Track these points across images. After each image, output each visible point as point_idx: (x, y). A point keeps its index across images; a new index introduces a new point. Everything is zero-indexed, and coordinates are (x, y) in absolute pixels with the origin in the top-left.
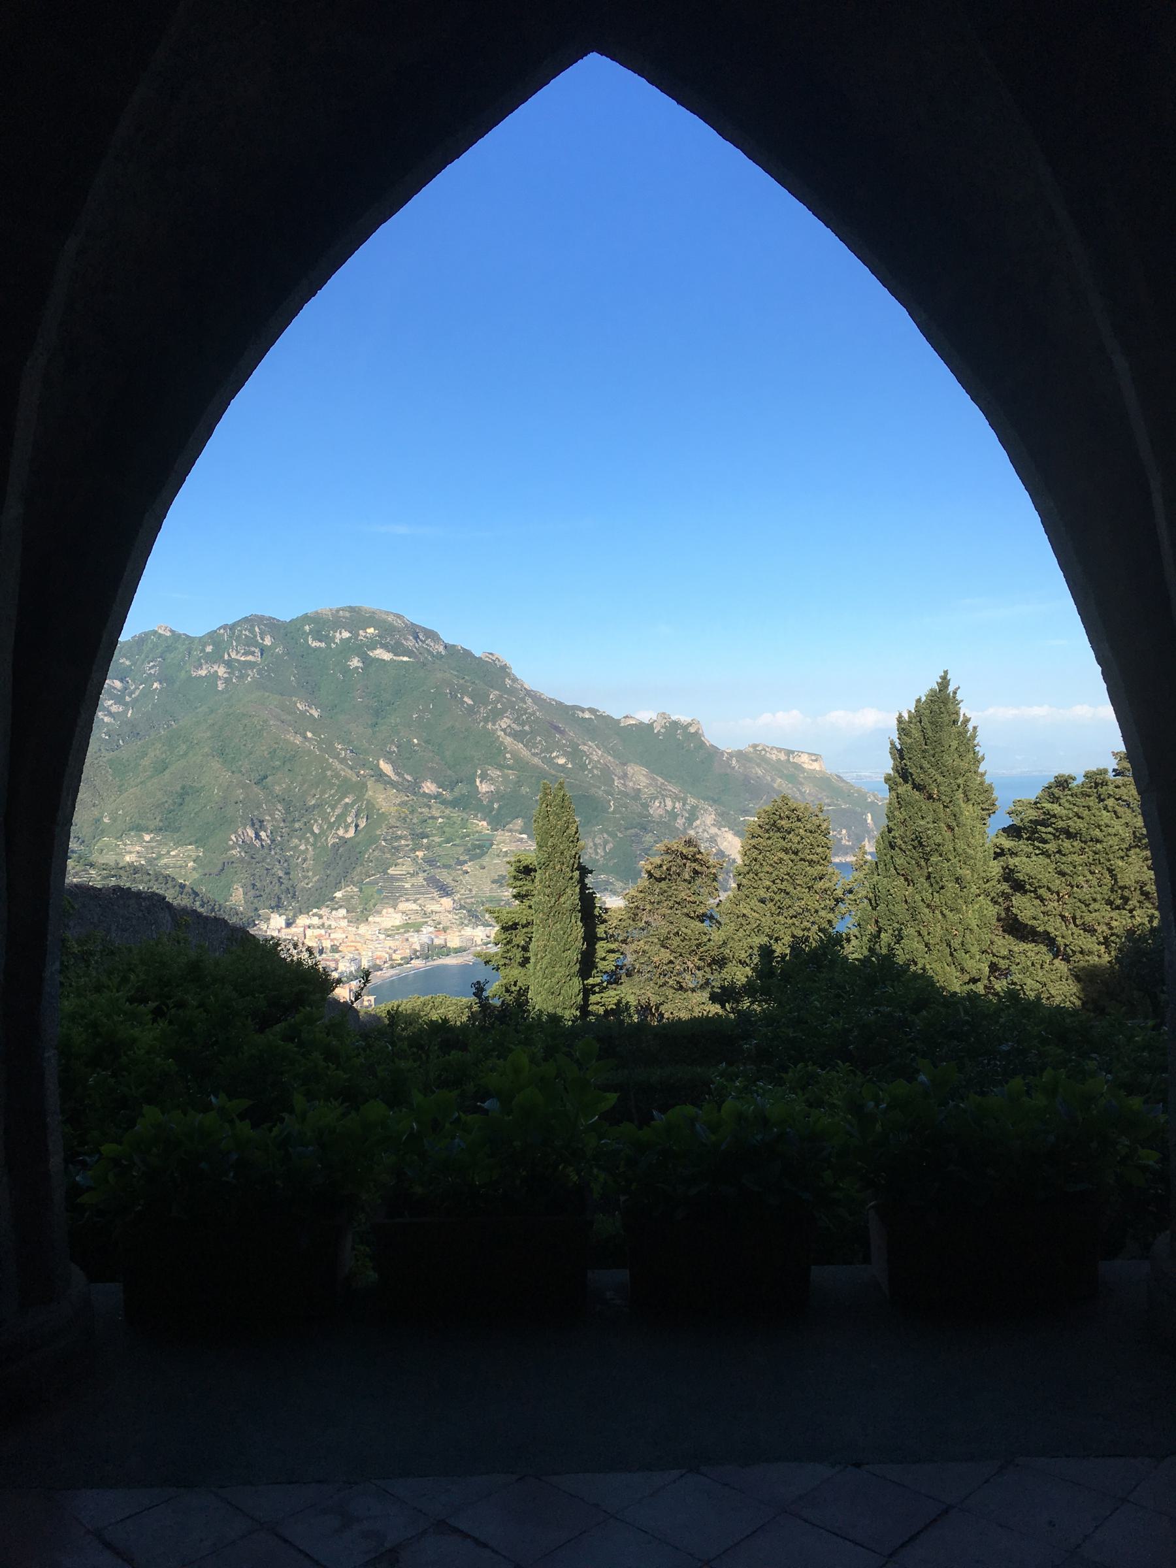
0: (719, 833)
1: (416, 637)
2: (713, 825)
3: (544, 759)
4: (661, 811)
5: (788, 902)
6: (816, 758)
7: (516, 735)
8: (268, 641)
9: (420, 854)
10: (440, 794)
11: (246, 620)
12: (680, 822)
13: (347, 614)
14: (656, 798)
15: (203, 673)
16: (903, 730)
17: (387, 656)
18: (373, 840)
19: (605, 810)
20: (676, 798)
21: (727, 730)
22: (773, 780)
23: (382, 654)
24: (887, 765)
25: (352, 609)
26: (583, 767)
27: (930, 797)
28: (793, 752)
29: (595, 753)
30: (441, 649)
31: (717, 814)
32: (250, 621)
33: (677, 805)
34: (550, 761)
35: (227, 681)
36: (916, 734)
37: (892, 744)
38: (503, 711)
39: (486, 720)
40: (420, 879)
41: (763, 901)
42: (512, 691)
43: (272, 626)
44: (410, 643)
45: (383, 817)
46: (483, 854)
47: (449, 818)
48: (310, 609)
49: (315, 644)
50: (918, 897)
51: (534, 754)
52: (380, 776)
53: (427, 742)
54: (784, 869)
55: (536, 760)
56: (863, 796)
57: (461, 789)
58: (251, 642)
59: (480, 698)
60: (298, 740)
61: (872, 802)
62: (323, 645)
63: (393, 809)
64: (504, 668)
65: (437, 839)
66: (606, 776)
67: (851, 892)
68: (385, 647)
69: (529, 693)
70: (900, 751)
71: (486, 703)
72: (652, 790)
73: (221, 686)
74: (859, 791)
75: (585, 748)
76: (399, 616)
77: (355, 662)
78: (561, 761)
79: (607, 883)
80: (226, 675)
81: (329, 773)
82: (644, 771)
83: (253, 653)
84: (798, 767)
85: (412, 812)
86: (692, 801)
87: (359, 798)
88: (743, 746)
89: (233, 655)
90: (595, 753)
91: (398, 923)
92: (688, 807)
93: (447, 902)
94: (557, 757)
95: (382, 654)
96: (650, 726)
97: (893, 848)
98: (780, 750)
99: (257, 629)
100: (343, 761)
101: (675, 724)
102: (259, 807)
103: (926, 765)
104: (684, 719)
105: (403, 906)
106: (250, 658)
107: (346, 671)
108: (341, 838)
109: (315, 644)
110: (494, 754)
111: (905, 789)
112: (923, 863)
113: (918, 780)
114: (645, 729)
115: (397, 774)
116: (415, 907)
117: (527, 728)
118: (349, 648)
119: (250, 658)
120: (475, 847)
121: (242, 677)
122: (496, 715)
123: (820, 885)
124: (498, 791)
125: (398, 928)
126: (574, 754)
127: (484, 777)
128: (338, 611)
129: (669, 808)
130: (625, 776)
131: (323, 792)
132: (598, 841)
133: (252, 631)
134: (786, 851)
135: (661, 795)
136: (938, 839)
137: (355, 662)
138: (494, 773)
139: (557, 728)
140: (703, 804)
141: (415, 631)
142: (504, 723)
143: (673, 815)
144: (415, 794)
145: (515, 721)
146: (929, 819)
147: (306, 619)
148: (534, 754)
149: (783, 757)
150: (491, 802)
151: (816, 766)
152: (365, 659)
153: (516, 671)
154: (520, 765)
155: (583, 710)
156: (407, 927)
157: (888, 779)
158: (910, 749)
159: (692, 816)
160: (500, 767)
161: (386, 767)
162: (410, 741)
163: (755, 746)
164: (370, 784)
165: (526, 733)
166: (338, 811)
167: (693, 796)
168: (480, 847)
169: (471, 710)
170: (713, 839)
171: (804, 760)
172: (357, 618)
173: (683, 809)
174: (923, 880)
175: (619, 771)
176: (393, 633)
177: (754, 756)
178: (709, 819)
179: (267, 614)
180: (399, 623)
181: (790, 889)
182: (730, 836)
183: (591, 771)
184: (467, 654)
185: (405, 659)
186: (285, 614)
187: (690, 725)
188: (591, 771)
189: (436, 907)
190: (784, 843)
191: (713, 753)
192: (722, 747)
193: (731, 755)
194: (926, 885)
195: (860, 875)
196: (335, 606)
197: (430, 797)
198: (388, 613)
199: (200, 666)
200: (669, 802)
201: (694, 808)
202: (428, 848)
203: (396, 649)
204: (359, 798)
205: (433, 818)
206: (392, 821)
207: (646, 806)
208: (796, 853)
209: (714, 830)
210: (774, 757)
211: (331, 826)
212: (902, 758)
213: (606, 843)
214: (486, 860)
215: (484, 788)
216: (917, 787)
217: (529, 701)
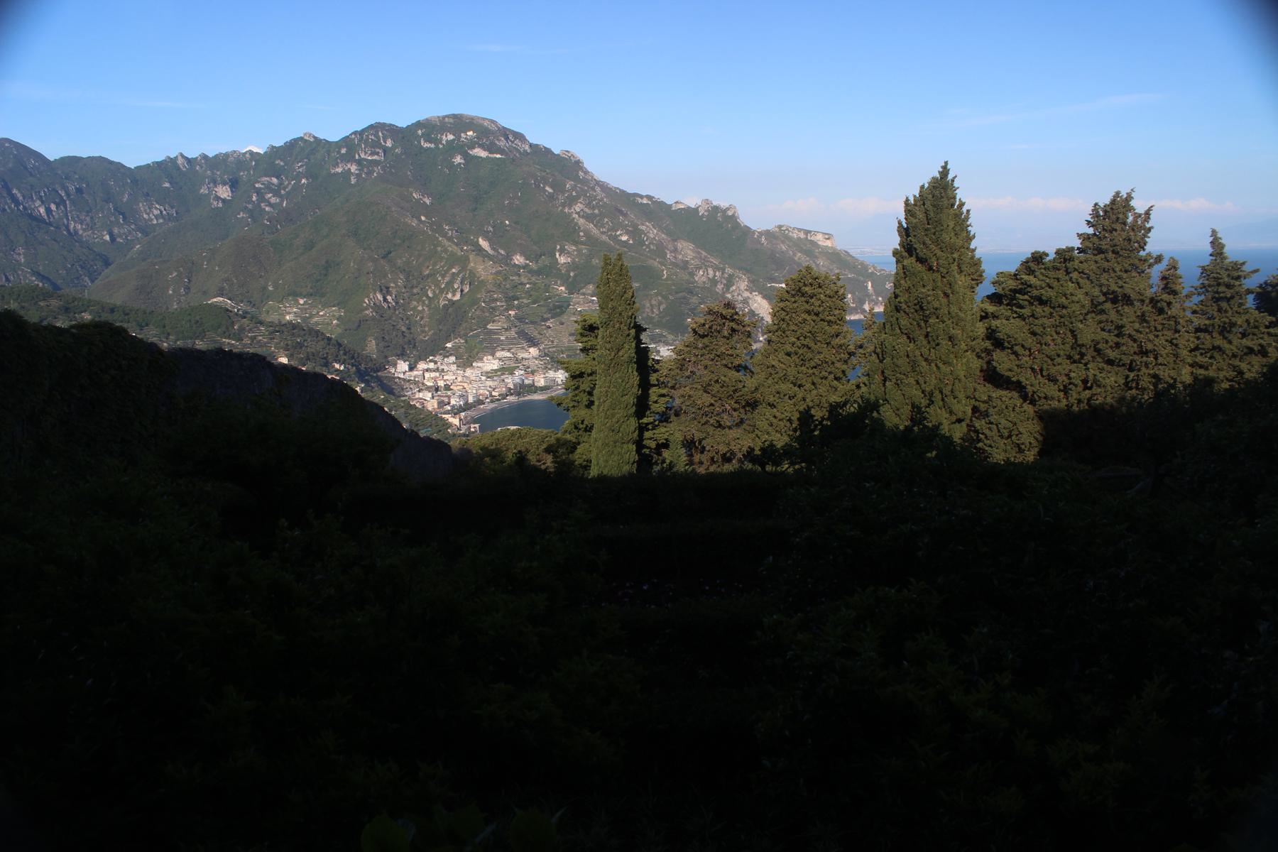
1: (507, 139)
3: (610, 237)
4: (704, 279)
5: (810, 355)
6: (829, 237)
7: (589, 218)
8: (389, 144)
9: (512, 313)
10: (527, 265)
11: (371, 127)
12: (720, 287)
15: (339, 170)
16: (909, 210)
17: (483, 154)
18: (475, 302)
19: (659, 276)
20: (716, 268)
21: (757, 215)
22: (795, 254)
23: (480, 152)
24: (895, 241)
25: (454, 116)
26: (642, 243)
27: (930, 269)
29: (651, 232)
30: (527, 148)
31: (749, 281)
32: (375, 128)
34: (615, 239)
35: (358, 176)
36: (921, 215)
37: (900, 223)
38: (578, 197)
39: (564, 205)
40: (513, 333)
41: (788, 354)
42: (584, 182)
43: (391, 130)
44: (502, 143)
45: (483, 283)
46: (562, 313)
47: (535, 284)
48: (422, 117)
49: (427, 145)
50: (917, 353)
51: (603, 233)
52: (480, 250)
53: (516, 223)
54: (807, 328)
55: (604, 238)
57: (544, 260)
58: (376, 144)
59: (559, 187)
63: (490, 277)
64: (578, 164)
65: (525, 301)
66: (660, 251)
67: (861, 347)
68: (482, 147)
69: (598, 183)
70: (907, 230)
71: (563, 191)
72: (697, 262)
73: (353, 181)
74: (862, 264)
75: (643, 228)
76: (493, 122)
77: (458, 160)
78: (624, 238)
82: (692, 246)
83: (377, 154)
84: (814, 243)
85: (505, 280)
86: (729, 270)
87: (464, 268)
88: (770, 226)
90: (651, 232)
91: (495, 367)
93: (534, 351)
95: (480, 152)
96: (696, 210)
97: (898, 311)
98: (800, 230)
100: (450, 239)
101: (716, 209)
102: (385, 276)
103: (928, 242)
105: (499, 354)
106: (375, 157)
107: (452, 166)
108: (450, 300)
109: (427, 145)
110: (570, 232)
111: (910, 261)
112: (923, 324)
113: (921, 254)
114: (691, 213)
115: (493, 249)
116: (508, 354)
118: (453, 148)
119: (375, 157)
120: (556, 307)
121: (370, 173)
122: (571, 201)
123: (837, 341)
124: (573, 262)
125: (496, 371)
126: (635, 232)
127: (562, 251)
128: (444, 117)
129: (711, 276)
130: (675, 250)
131: (435, 264)
132: (654, 302)
134: (809, 312)
135: (704, 265)
136: (936, 304)
137: (458, 160)
138: (570, 248)
139: (621, 212)
141: (506, 133)
142: (578, 207)
143: (714, 282)
144: (507, 265)
145: (588, 205)
146: (930, 287)
147: (419, 124)
148: (603, 233)
149: (802, 236)
150: (568, 271)
151: (828, 243)
152: (466, 156)
153: (589, 165)
154: (591, 241)
155: (641, 197)
156: (503, 370)
157: (895, 253)
158: (915, 228)
159: (730, 282)
160: (575, 243)
161: (483, 243)
162: (503, 223)
163: (780, 227)
164: (471, 257)
165: (596, 216)
166: (447, 279)
168: (560, 307)
169: (551, 197)
170: (746, 301)
171: (819, 239)
172: (459, 123)
173: (722, 277)
174: (922, 338)
175: (670, 246)
176: (489, 133)
177: (778, 235)
178: (743, 285)
179: (388, 122)
180: (493, 127)
181: (812, 344)
182: (759, 299)
183: (648, 246)
184: (548, 151)
186: (403, 122)
187: (728, 209)
188: (648, 246)
189: (525, 355)
190: (807, 306)
191: (747, 231)
192: (753, 227)
193: (761, 233)
194: (925, 342)
195: (869, 333)
196: (442, 114)
197: (519, 267)
198: (484, 119)
199: (337, 165)
200: (711, 272)
202: (519, 307)
203: (491, 148)
204: (464, 268)
205: (522, 284)
206: (490, 287)
207: (692, 274)
208: (817, 314)
209: (746, 294)
211: (442, 291)
212: (908, 235)
213: (660, 303)
214: (564, 318)
215: (562, 260)
216: (921, 260)
217: (598, 189)
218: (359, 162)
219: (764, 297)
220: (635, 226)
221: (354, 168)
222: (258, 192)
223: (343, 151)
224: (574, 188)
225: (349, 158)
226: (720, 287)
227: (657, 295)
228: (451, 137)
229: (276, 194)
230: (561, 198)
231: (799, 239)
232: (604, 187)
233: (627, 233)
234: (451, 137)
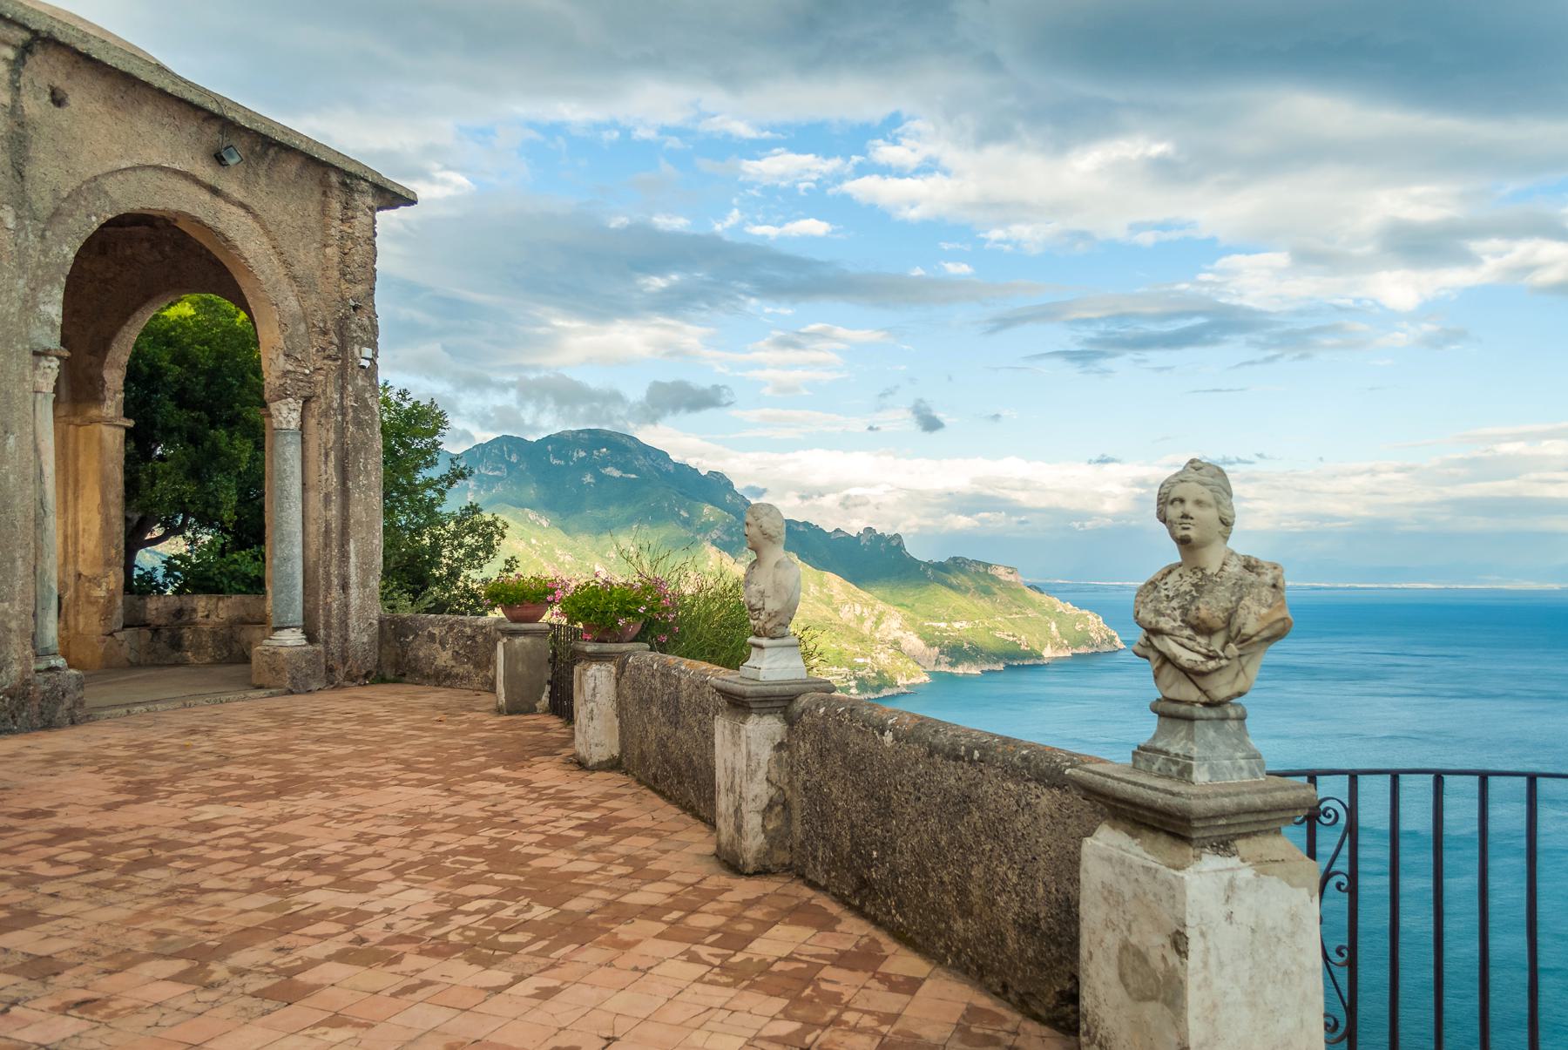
4: (850, 615)
8: (514, 459)
12: (868, 624)
14: (844, 603)
17: (617, 473)
68: (617, 466)
77: (588, 478)
86: (880, 606)
133: (501, 450)
140: (892, 609)
143: (861, 619)
151: (1012, 578)
159: (879, 621)
203: (623, 468)
207: (836, 610)
226: (868, 624)
228: (582, 454)
234: (582, 454)
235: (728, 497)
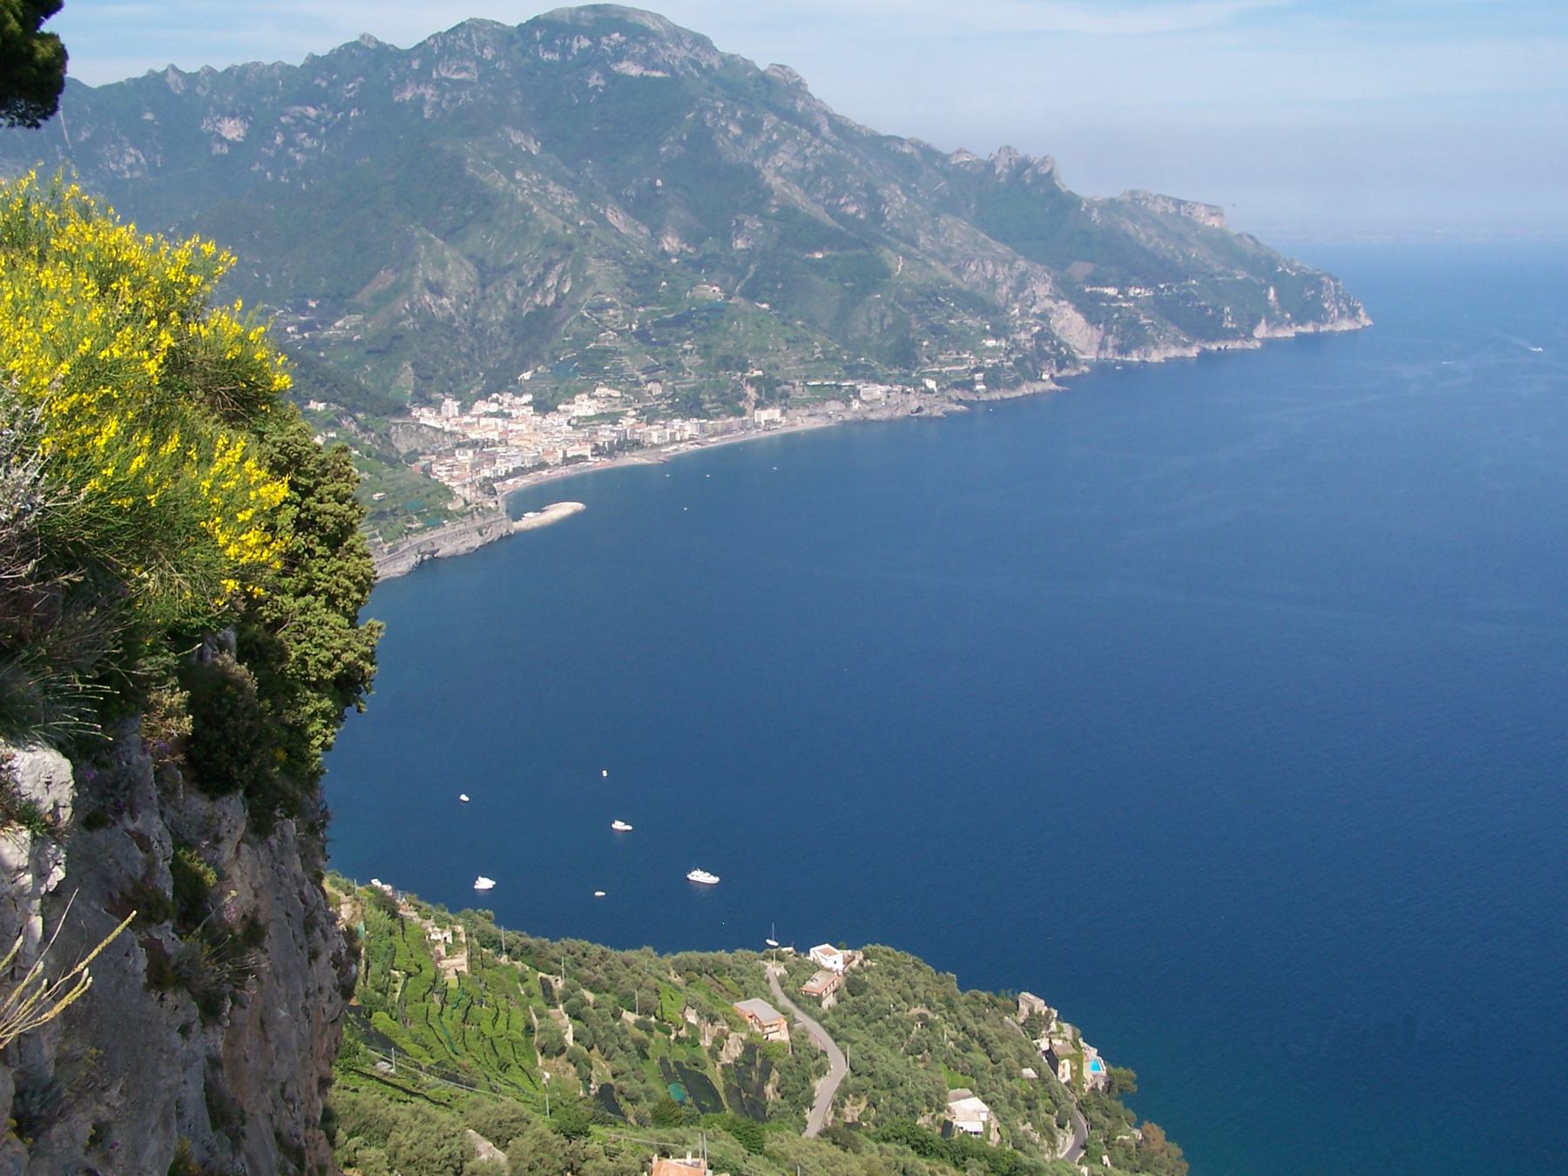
0: (1055, 307)
2: (1048, 297)
6: (1215, 211)
13: (591, 16)
15: (408, 96)
17: (634, 70)
25: (595, 7)
26: (878, 218)
28: (1184, 203)
29: (896, 201)
31: (1055, 282)
33: (1000, 270)
49: (548, 56)
51: (817, 202)
55: (819, 212)
56: (1272, 262)
60: (501, 183)
61: (1284, 272)
62: (557, 57)
69: (833, 120)
76: (659, 17)
78: (852, 209)
79: (866, 367)
80: (435, 99)
81: (531, 224)
83: (466, 69)
84: (1189, 222)
86: (1022, 264)
89: (443, 74)
92: (1015, 273)
94: (846, 204)
96: (990, 166)
98: (1166, 199)
99: (474, 37)
101: (1025, 164)
104: (1035, 156)
106: (463, 75)
109: (548, 56)
117: (810, 165)
118: (589, 60)
119: (463, 75)
122: (771, 149)
126: (874, 200)
128: (580, 9)
130: (935, 231)
132: (873, 314)
133: (468, 39)
137: (596, 80)
141: (678, 35)
142: (781, 159)
147: (536, 23)
151: (1214, 222)
152: (607, 73)
153: (816, 89)
154: (789, 213)
155: (901, 141)
163: (1133, 193)
167: (1028, 256)
171: (1201, 215)
178: (1042, 289)
185: (658, 74)
187: (1043, 162)
191: (1069, 203)
193: (1092, 205)
198: (643, 13)
201: (1023, 274)
203: (647, 61)
209: (1049, 304)
210: (1159, 209)
213: (883, 316)
217: (825, 129)
218: (439, 84)
219: (1079, 308)
220: (870, 188)
221: (429, 93)
222: (285, 130)
223: (415, 65)
224: (775, 128)
225: (423, 76)
227: (879, 302)
228: (586, 43)
229: (312, 133)
230: (755, 145)
231: (1165, 213)
232: (840, 127)
233: (858, 200)
234: (586, 43)
235: (800, 105)
